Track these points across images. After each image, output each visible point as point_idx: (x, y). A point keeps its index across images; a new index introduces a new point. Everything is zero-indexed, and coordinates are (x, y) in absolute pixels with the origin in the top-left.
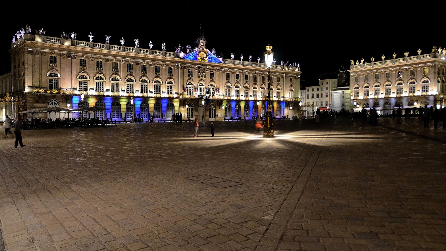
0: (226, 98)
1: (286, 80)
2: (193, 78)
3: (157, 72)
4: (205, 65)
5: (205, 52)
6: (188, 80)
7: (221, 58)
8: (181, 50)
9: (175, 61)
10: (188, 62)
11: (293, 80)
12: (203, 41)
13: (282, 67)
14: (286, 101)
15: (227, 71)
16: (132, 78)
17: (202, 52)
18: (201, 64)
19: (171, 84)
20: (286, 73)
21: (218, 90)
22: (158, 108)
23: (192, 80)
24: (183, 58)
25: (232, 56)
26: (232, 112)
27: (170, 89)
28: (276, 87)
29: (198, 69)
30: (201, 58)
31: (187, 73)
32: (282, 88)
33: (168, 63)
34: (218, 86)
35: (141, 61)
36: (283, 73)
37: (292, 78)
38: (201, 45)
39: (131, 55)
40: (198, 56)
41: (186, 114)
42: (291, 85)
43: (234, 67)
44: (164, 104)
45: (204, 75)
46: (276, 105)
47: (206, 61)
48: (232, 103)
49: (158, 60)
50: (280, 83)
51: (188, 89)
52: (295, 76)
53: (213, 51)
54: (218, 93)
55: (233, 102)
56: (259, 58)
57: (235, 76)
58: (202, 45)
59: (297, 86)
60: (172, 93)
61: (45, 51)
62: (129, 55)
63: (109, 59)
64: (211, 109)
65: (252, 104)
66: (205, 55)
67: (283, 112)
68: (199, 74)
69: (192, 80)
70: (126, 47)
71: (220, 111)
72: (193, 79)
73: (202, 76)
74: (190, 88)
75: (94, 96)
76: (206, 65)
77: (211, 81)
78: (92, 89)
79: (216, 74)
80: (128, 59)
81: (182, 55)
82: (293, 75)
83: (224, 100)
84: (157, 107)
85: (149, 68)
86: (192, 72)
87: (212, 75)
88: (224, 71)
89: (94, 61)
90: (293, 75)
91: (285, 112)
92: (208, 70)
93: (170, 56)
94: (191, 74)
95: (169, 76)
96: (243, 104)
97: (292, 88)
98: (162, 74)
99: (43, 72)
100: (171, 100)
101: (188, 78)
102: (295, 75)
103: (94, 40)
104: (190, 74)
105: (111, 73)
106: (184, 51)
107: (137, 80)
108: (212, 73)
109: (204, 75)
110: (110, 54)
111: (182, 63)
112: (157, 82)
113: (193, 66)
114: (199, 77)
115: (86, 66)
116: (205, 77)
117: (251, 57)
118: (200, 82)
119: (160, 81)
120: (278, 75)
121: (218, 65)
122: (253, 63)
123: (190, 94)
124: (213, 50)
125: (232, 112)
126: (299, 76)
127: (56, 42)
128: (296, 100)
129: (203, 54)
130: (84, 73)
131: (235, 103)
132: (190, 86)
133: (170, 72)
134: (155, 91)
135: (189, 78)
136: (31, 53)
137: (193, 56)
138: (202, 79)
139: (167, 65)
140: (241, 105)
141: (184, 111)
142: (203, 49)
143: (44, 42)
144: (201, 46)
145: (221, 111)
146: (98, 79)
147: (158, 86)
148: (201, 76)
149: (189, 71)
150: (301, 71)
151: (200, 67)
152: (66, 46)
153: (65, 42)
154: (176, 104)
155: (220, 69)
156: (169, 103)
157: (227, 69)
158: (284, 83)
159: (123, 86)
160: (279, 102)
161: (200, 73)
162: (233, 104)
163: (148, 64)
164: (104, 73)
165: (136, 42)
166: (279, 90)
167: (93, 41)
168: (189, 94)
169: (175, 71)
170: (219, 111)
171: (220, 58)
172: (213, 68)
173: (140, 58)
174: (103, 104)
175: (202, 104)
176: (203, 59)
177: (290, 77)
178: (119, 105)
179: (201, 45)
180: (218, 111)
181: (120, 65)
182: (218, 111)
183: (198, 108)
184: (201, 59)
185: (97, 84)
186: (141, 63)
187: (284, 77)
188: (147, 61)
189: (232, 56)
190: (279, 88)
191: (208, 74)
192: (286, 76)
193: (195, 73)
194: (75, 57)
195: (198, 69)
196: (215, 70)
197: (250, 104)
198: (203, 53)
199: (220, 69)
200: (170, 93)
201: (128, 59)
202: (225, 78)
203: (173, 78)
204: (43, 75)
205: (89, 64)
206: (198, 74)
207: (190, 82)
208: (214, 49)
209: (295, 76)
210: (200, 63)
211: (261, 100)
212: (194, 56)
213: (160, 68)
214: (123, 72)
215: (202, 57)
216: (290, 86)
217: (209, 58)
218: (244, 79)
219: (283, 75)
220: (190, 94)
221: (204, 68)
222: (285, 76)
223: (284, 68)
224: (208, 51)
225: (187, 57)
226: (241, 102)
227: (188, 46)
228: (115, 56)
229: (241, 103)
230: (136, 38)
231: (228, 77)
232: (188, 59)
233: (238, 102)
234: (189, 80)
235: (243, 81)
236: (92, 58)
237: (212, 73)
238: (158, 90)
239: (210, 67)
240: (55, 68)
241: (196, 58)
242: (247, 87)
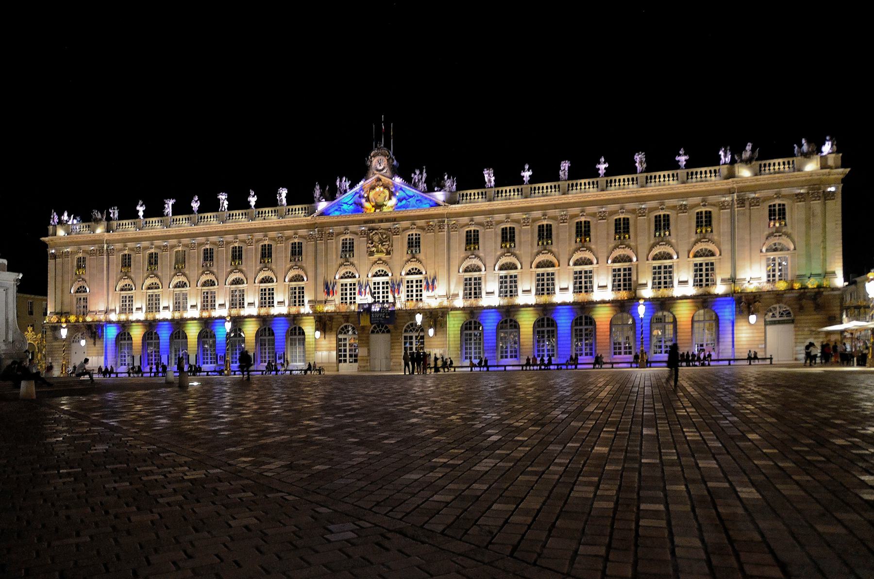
0: (459, 303)
1: (744, 214)
2: (421, 256)
3: (471, 243)
4: (388, 220)
5: (386, 187)
6: (341, 265)
7: (440, 191)
8: (321, 195)
9: (307, 224)
10: (339, 222)
12: (382, 157)
13: (724, 170)
15: (467, 225)
16: (711, 247)
17: (377, 189)
18: (377, 221)
19: (299, 281)
20: (741, 190)
21: (433, 282)
22: (548, 331)
23: (352, 264)
24: (323, 214)
25: (489, 176)
26: (487, 345)
27: (297, 295)
28: (687, 249)
29: (368, 235)
30: (373, 204)
31: (336, 248)
33: (289, 233)
34: (431, 273)
35: (229, 238)
36: (730, 191)
38: (378, 170)
39: (206, 231)
40: (363, 200)
41: (334, 353)
43: (493, 210)
44: (280, 330)
45: (386, 247)
46: (687, 312)
47: (391, 209)
48: (484, 318)
49: (265, 230)
51: (387, 288)
52: (802, 191)
53: (416, 177)
54: (433, 290)
55: (489, 314)
56: (252, 193)
57: (496, 234)
58: (381, 168)
59: (816, 232)
60: (301, 303)
61: (69, 250)
62: (202, 231)
63: (167, 246)
64: (470, 335)
65: (568, 314)
66: (387, 192)
67: (730, 336)
68: (370, 246)
69: (352, 264)
70: (763, 162)
71: (490, 341)
72: (355, 262)
73: (382, 252)
74: (348, 287)
75: (608, 302)
76: (394, 220)
77: (408, 261)
78: (683, 283)
79: (426, 239)
80: (202, 239)
81: (322, 205)
82: (785, 191)
83: (110, 322)
84: (546, 329)
85: (246, 250)
86: (352, 244)
87: (414, 244)
88: (455, 227)
89: (531, 226)
91: (735, 336)
92: (397, 232)
93: (298, 215)
94: (350, 251)
95: (293, 264)
96: (527, 316)
98: (276, 261)
99: (67, 285)
100: (293, 322)
101: (340, 261)
102: (802, 187)
103: (291, 200)
104: (348, 248)
105: (173, 273)
106: (331, 196)
107: (526, 265)
108: (414, 237)
109: (386, 247)
110: (167, 236)
111: (322, 226)
112: (622, 259)
113: (353, 228)
114: (371, 254)
115: (130, 266)
116: (388, 253)
117: (565, 165)
118: (376, 269)
119: (590, 258)
121: (350, 219)
122: (760, 162)
123: (348, 302)
124: (415, 174)
125: (487, 345)
126: (832, 189)
127: (711, 176)
128: (81, 320)
129: (383, 192)
130: (126, 280)
131: (494, 317)
132: (349, 281)
133: (704, 221)
134: (271, 300)
135: (342, 260)
136: (54, 256)
137: (351, 204)
138: (380, 259)
139: (288, 238)
140: (523, 319)
141: (328, 346)
142: (379, 180)
143: (756, 175)
144: (376, 172)
145: (442, 343)
146: (152, 288)
147: (269, 290)
148: (377, 252)
149: (343, 243)
150: (843, 166)
151: (371, 229)
152: (811, 174)
153: (804, 164)
154: (309, 328)
155: (102, 250)
156: (581, 318)
157: (465, 220)
159: (194, 299)
160: (704, 301)
161: (372, 243)
162: (487, 321)
163: (244, 241)
164: (159, 274)
165: (223, 197)
166: (707, 256)
167: (229, 209)
168: (346, 303)
169: (308, 249)
170: (437, 343)
171: (437, 191)
172: (296, 234)
173: (227, 233)
174: (552, 323)
175: (416, 324)
176: (379, 206)
178: (516, 326)
179: (378, 170)
180: (433, 343)
181: (636, 221)
182: (433, 343)
183: (368, 337)
184: (373, 206)
185: (468, 282)
186: (228, 243)
187: (731, 206)
188: (242, 236)
189: (489, 176)
191: (400, 244)
192: (742, 202)
193: (361, 245)
194: (109, 253)
195: (367, 235)
196: (422, 228)
197: (558, 315)
198: (382, 189)
199: (439, 222)
200: (297, 304)
201: (202, 239)
202: (460, 245)
203: (304, 265)
204: (66, 292)
205: (134, 261)
206: (369, 247)
207: (348, 270)
208: (418, 172)
210: (371, 217)
211: (530, 303)
212: (355, 203)
213: (631, 222)
214: (194, 268)
215: (380, 200)
217: (400, 200)
218: (532, 238)
220: (348, 302)
221: (387, 229)
223: (731, 175)
224: (398, 180)
225: (336, 210)
226: (518, 311)
227: (338, 180)
228: (179, 237)
229: (521, 316)
230: (488, 168)
231: (472, 240)
232: (337, 213)
233: (178, 326)
234: (772, 238)
235: (532, 245)
236: (489, 225)
237: (414, 237)
238: (269, 298)
239: (406, 224)
240: (83, 276)
241: (358, 207)
242: (551, 262)
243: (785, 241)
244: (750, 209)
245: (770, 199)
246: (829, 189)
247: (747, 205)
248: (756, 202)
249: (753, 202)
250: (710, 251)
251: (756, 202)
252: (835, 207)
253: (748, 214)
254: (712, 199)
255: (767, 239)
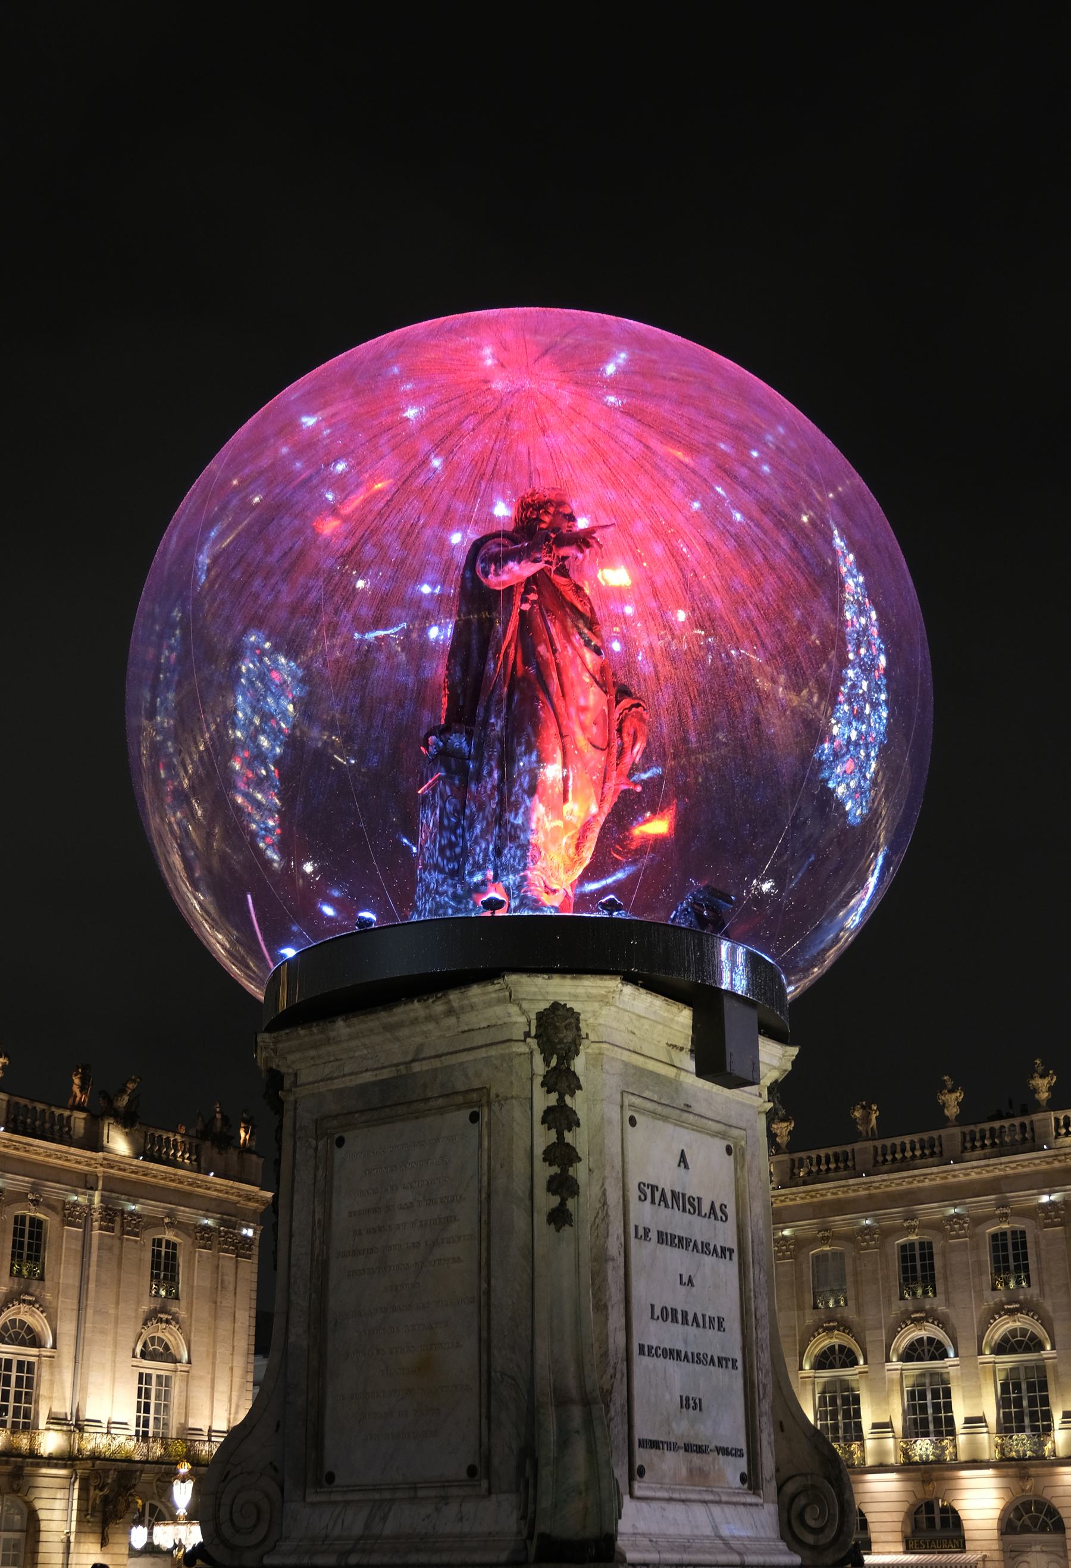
11: (190, 1262)
14: (95, 1456)
32: (67, 1328)
36: (86, 1182)
37: (169, 1235)
42: (164, 1310)
50: (42, 1278)
52: (209, 1222)
59: (225, 1325)
82: (185, 1213)
90: (185, 1213)
97: (167, 1337)
102: (208, 1212)
120: (19, 1197)
126: (250, 1233)
158: (84, 1279)
166: (22, 1343)
177: (155, 1223)
190: (29, 1320)
192: (111, 1214)
209: (206, 1228)
216: (151, 1317)
219: (75, 1204)
222: (96, 1215)
223: (94, 1142)
243: (173, 1338)
244: (121, 1239)
245: (156, 1225)
246: (244, 1232)
247: (117, 1227)
248: (134, 1225)
249: (129, 1224)
250: (30, 1330)
251: (134, 1225)
252: (249, 1269)
253: (116, 1251)
254: (53, 1190)
255: (145, 1324)
